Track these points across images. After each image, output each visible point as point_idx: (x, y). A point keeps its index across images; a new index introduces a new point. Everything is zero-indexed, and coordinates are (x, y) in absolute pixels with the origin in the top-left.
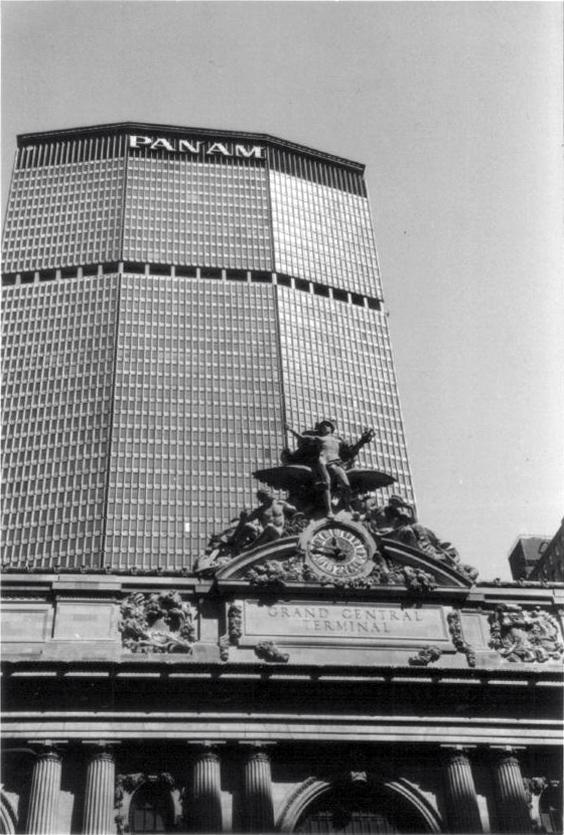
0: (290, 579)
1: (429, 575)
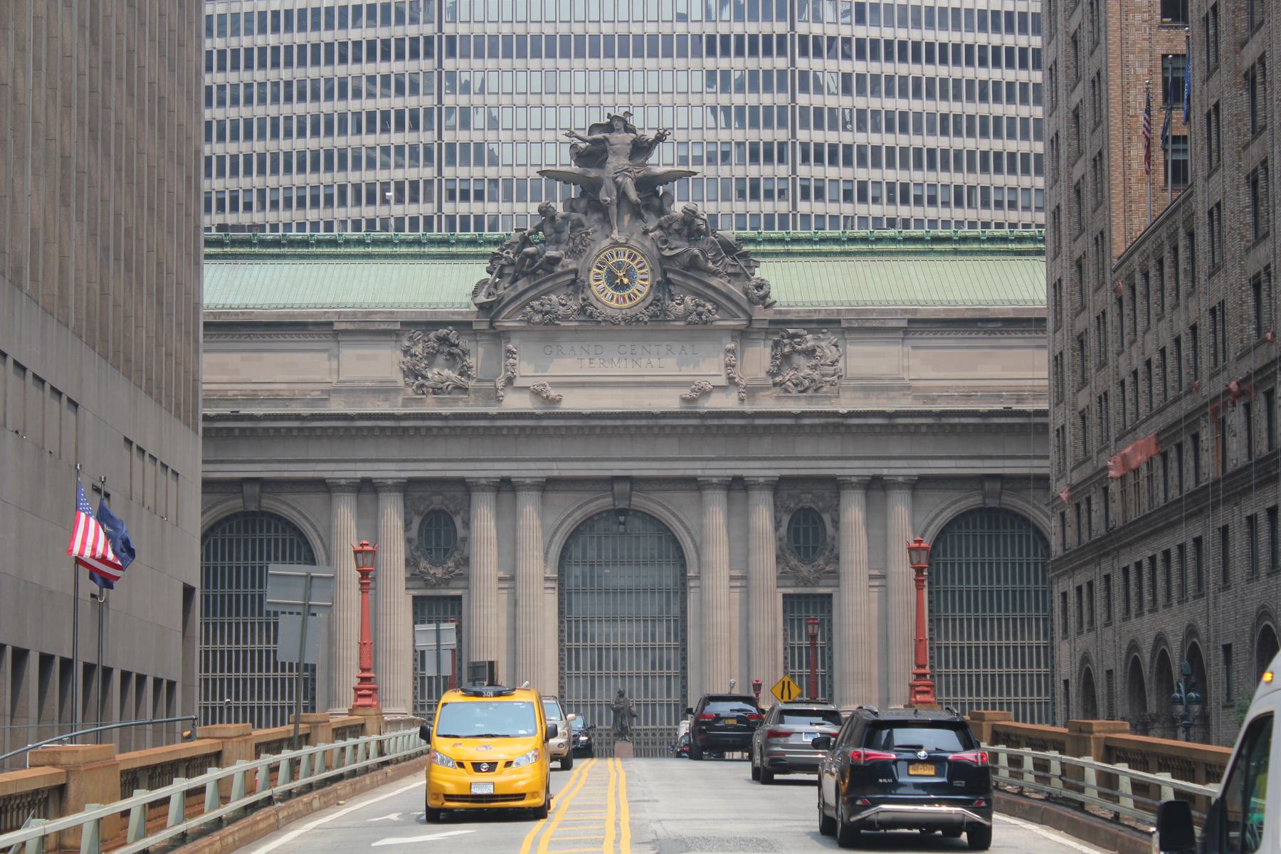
0: (566, 318)
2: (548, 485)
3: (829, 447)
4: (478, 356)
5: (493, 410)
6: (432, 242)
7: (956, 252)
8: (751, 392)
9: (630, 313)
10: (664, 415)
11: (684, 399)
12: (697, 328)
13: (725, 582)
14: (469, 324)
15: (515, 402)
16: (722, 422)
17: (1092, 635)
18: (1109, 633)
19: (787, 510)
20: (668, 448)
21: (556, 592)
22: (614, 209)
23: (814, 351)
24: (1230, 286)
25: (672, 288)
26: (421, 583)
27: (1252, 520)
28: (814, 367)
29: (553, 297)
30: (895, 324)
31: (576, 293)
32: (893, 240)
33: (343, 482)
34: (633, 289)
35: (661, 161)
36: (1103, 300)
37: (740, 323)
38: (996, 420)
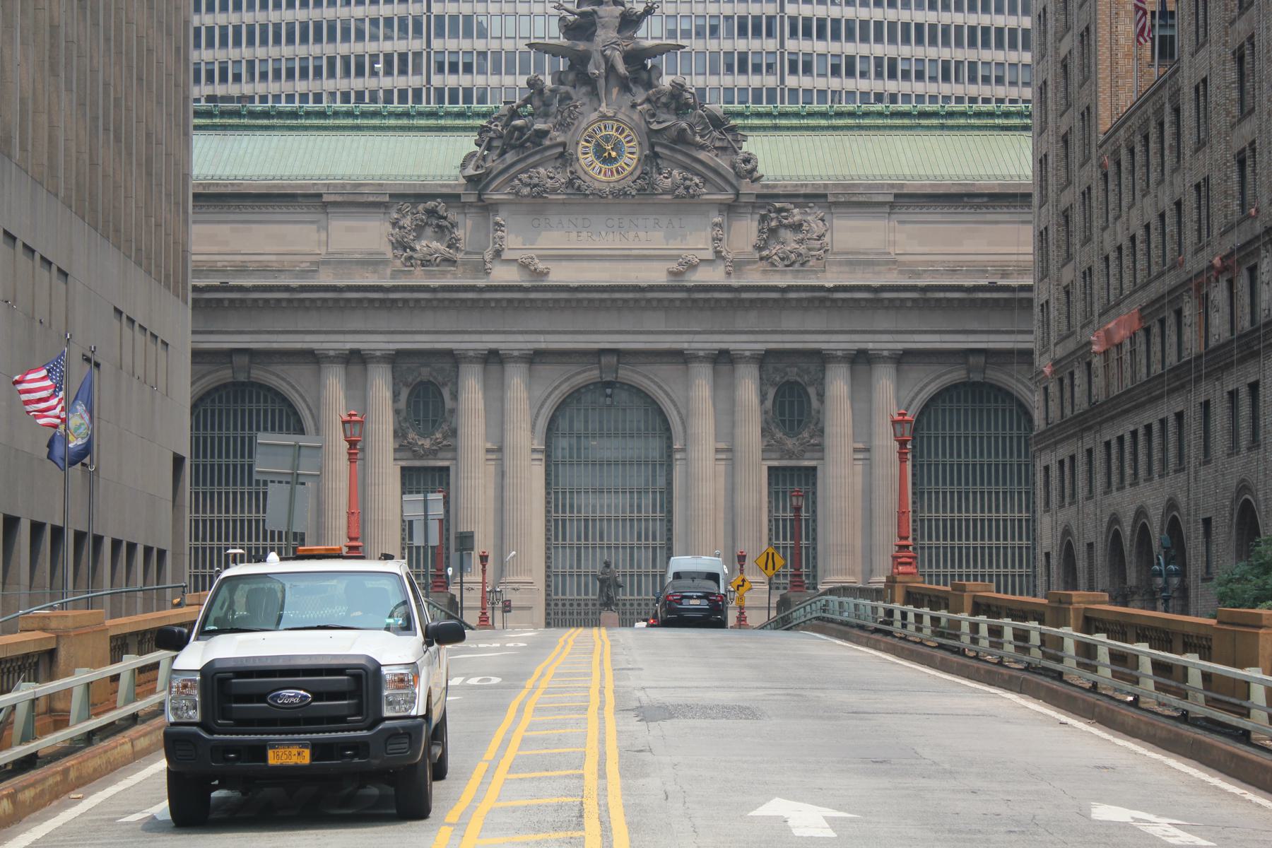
0: (554, 191)
1: (696, 180)
2: (536, 358)
3: (815, 321)
4: (466, 228)
5: (481, 283)
6: (421, 114)
7: (942, 127)
8: (738, 266)
9: (618, 186)
10: (652, 288)
11: (671, 273)
12: (685, 201)
13: (711, 454)
14: (458, 196)
15: (503, 274)
16: (709, 295)
17: (1074, 508)
18: (1090, 507)
19: (773, 384)
20: (654, 320)
21: (543, 463)
22: (602, 82)
23: (801, 225)
24: (1215, 161)
25: (659, 161)
26: (409, 454)
27: (1233, 395)
28: (801, 242)
29: (542, 170)
30: (881, 199)
31: (564, 166)
32: (880, 115)
33: (332, 353)
34: (621, 163)
35: (649, 34)
36: (1090, 175)
37: (727, 196)
38: (981, 295)
